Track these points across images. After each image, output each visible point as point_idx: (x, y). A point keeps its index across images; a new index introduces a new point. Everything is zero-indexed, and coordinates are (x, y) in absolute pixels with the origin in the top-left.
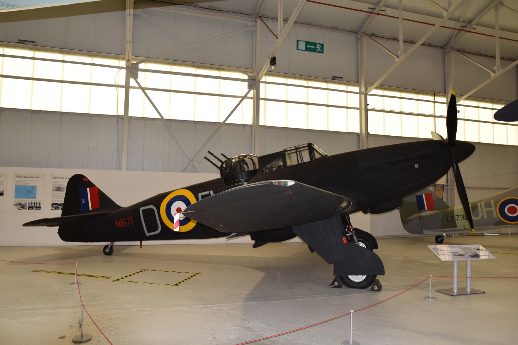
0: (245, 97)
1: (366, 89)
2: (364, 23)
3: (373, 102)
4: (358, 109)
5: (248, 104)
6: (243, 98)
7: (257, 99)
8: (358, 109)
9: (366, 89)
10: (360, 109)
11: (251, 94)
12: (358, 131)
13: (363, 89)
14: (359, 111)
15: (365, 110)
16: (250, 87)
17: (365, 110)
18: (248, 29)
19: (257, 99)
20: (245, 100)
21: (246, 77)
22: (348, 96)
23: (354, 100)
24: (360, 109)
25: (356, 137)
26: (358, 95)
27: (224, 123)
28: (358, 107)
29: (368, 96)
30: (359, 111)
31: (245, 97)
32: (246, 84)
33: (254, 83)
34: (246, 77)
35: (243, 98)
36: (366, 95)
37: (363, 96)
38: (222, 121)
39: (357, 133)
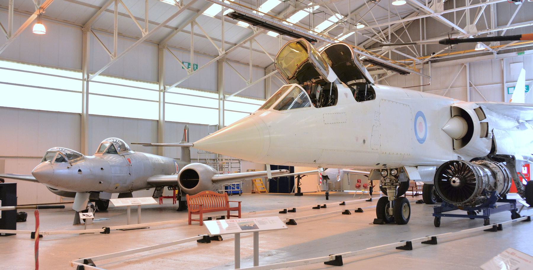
1: (88, 77)
2: (89, 19)
4: (81, 92)
8: (81, 92)
9: (88, 77)
10: (82, 92)
12: (80, 112)
13: (86, 76)
14: (81, 94)
22: (72, 80)
23: (78, 85)
24: (82, 92)
25: (78, 116)
26: (82, 81)
29: (90, 82)
30: (81, 94)
36: (88, 82)
37: (85, 82)
39: (79, 114)
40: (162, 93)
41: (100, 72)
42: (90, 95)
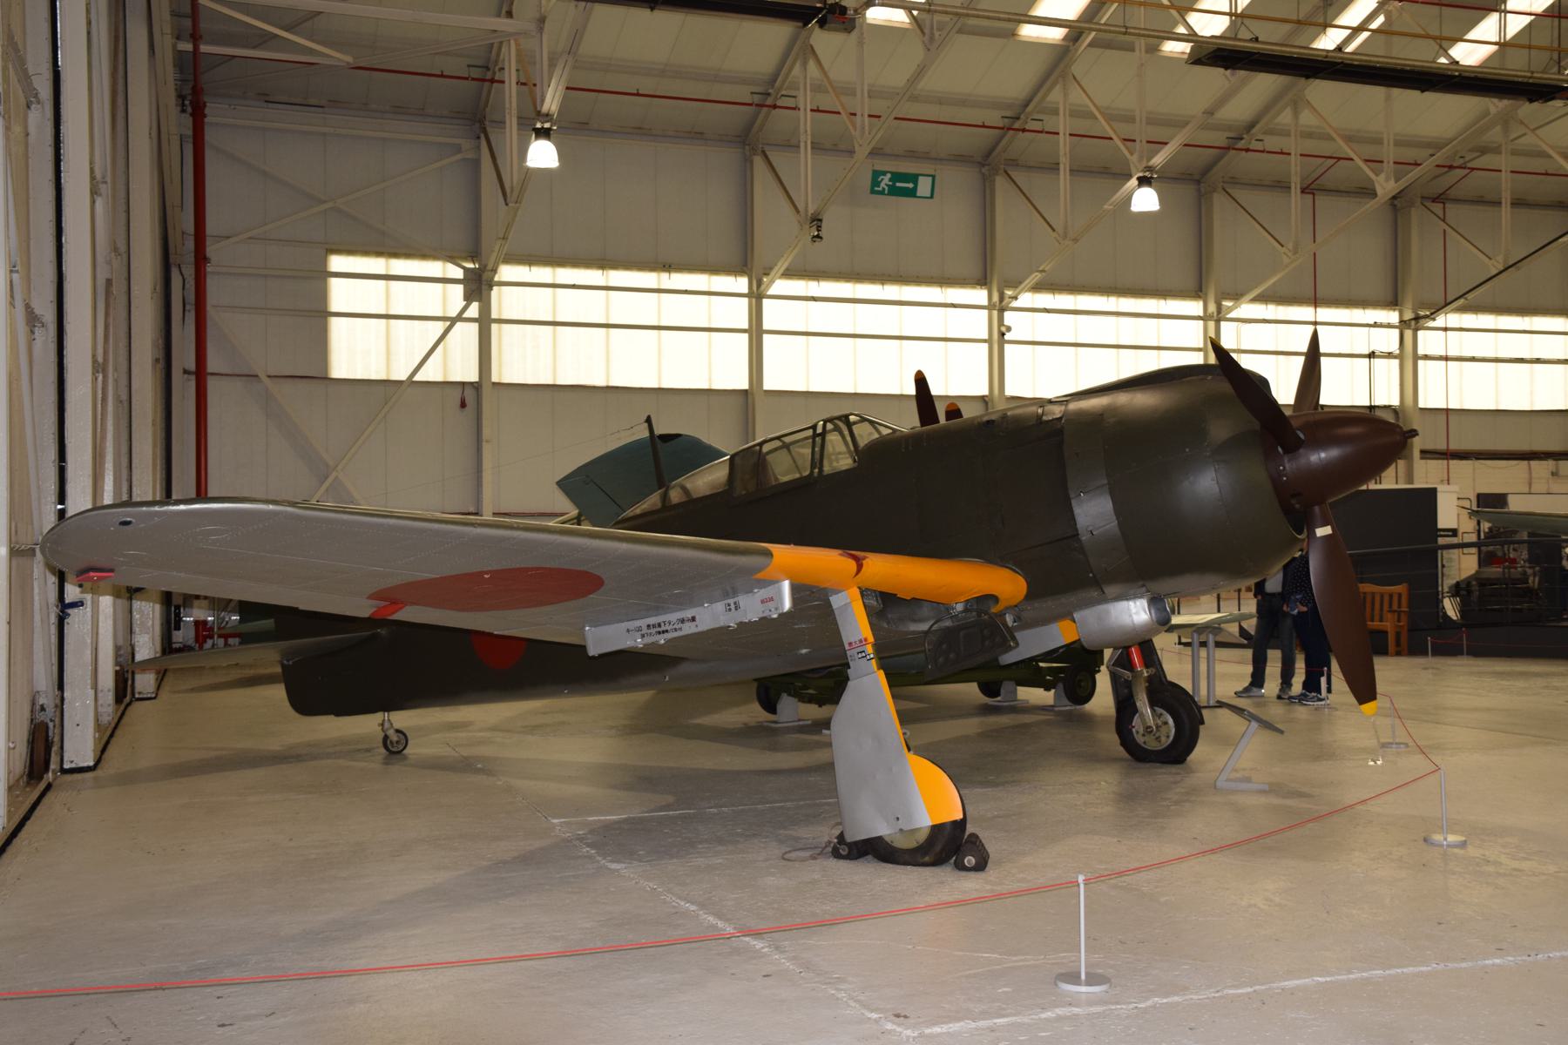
0: (460, 318)
3: (774, 314)
5: (466, 335)
6: (453, 321)
7: (485, 322)
11: (474, 310)
14: (746, 336)
15: (756, 332)
16: (469, 298)
17: (756, 332)
18: (459, 157)
19: (485, 322)
20: (459, 325)
21: (458, 273)
27: (410, 382)
28: (746, 326)
29: (765, 302)
31: (460, 318)
32: (460, 288)
33: (478, 286)
34: (458, 273)
35: (453, 321)
38: (403, 376)
40: (995, 313)
41: (782, 266)
42: (765, 337)
